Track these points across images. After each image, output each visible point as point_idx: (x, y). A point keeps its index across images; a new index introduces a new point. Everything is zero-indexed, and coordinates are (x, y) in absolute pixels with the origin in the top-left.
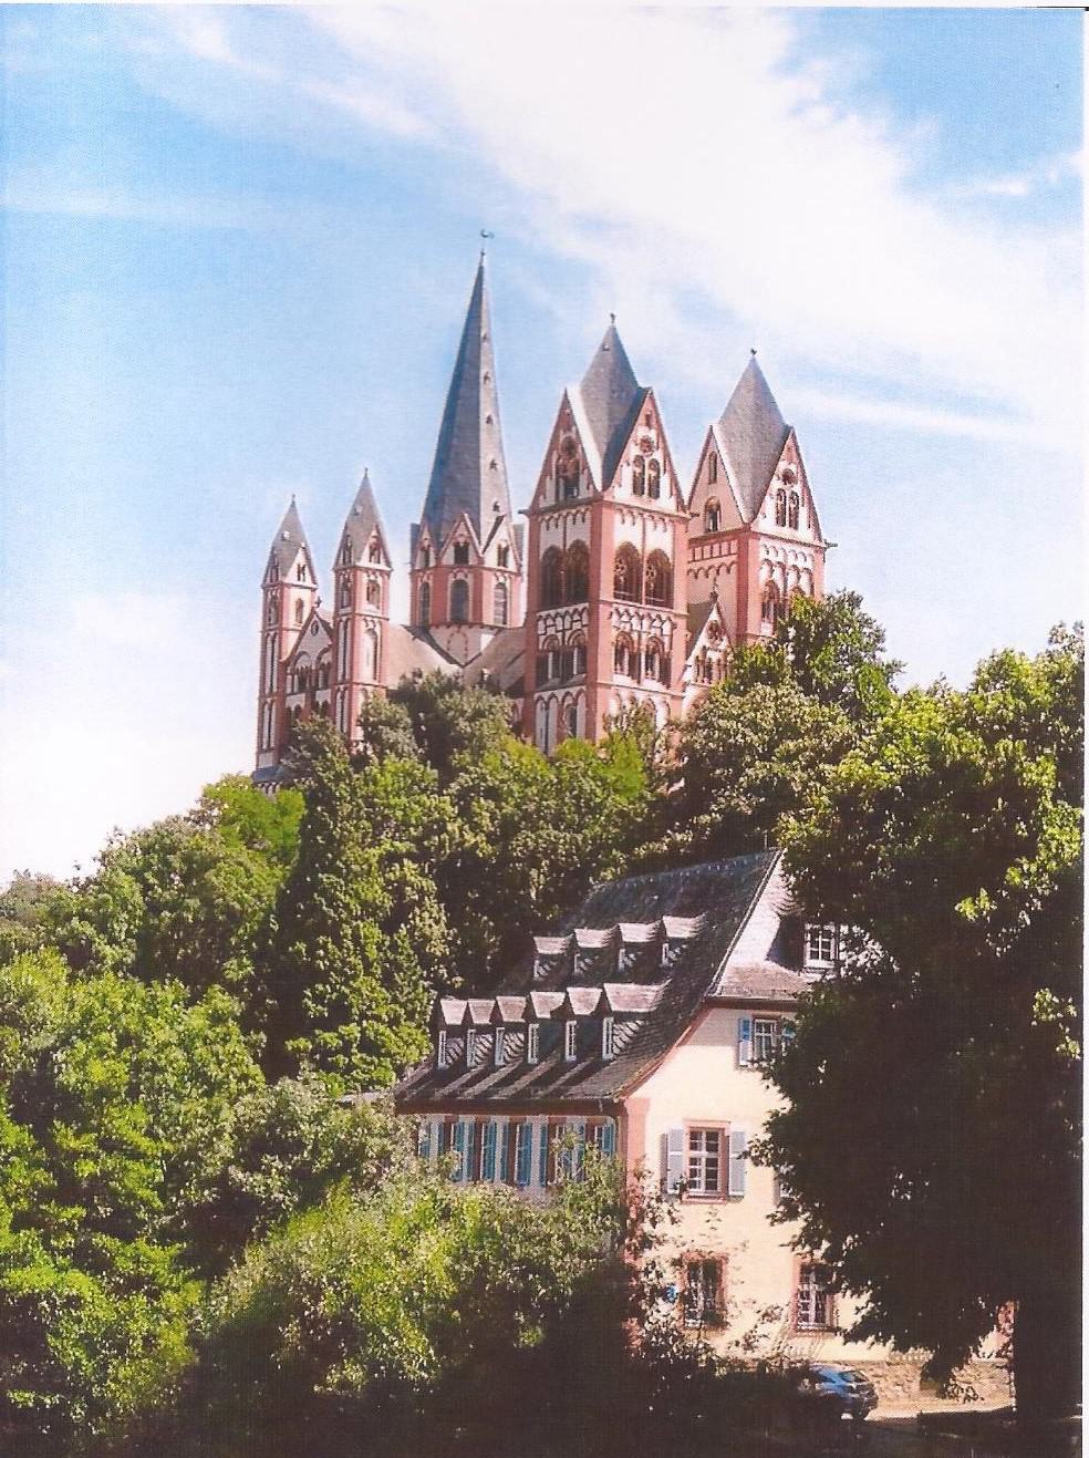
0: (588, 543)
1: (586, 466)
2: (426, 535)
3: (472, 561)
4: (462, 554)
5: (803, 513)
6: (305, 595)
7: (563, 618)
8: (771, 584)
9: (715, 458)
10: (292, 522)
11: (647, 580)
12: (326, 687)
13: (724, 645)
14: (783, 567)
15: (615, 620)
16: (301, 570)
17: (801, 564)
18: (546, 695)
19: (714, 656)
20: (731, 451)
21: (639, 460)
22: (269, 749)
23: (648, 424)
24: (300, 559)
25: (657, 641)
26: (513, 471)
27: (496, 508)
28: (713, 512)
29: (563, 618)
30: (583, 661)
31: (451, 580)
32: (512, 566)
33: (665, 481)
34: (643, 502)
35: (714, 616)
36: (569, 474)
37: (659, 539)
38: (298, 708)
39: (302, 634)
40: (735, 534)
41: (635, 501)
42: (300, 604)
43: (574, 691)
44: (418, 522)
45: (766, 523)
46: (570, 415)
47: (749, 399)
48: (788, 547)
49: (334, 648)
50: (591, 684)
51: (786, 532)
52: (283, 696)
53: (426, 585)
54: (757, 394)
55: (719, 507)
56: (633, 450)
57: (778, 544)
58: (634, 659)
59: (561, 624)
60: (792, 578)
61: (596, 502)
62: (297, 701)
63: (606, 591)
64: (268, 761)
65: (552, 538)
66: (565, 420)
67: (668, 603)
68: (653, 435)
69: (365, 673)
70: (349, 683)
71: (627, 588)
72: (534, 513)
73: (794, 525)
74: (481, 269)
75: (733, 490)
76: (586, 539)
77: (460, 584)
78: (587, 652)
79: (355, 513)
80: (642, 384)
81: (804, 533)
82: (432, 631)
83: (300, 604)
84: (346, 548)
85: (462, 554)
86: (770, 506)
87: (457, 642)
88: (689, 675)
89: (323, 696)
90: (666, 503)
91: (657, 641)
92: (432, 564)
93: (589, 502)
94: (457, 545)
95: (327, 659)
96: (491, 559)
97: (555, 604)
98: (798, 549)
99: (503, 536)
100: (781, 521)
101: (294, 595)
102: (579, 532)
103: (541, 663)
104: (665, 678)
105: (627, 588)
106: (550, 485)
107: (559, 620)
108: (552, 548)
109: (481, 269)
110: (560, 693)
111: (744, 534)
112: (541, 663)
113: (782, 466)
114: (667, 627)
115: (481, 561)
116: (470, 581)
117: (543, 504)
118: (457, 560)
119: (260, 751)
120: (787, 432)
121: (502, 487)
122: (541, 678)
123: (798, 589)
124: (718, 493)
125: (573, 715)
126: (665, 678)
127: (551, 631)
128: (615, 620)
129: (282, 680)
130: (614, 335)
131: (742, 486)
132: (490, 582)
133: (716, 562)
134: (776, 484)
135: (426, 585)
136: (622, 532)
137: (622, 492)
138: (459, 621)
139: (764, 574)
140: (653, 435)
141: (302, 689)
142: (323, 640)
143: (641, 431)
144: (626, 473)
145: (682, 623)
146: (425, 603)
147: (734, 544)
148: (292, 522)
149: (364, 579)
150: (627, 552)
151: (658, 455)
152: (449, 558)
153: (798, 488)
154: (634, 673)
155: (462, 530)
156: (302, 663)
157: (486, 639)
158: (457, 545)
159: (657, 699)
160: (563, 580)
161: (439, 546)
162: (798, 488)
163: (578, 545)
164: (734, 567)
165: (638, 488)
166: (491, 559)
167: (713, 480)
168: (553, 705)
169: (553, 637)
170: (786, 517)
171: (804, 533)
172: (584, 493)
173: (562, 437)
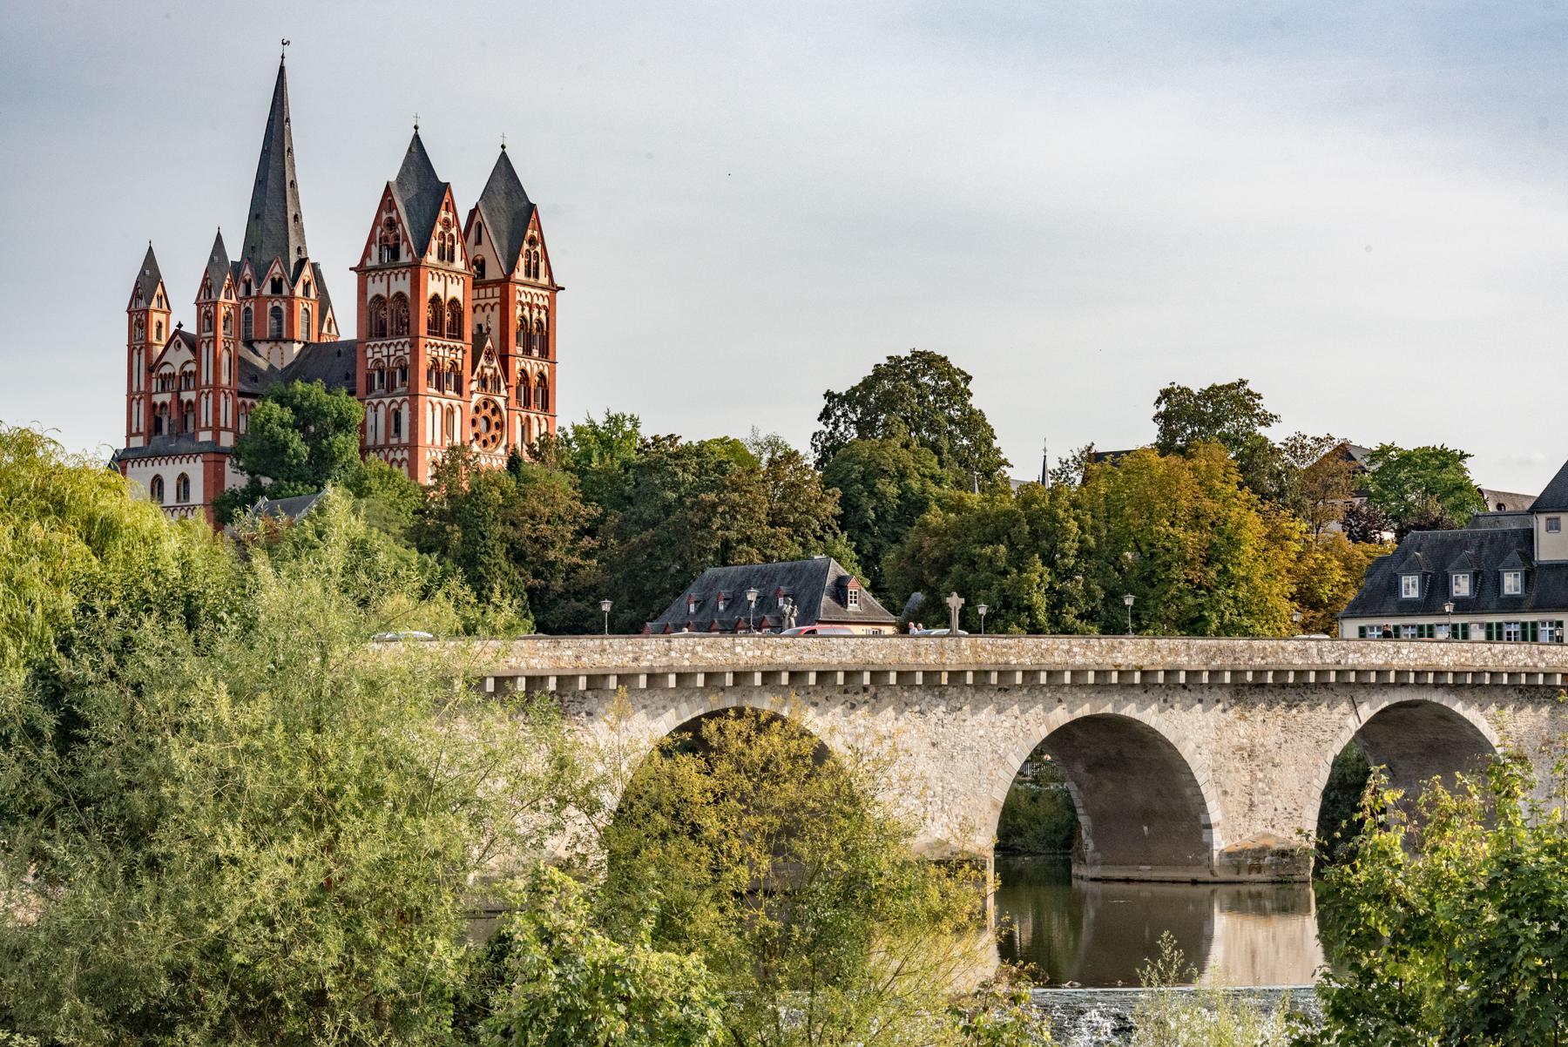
0: (407, 292)
1: (406, 239)
2: (247, 271)
3: (286, 292)
5: (542, 265)
6: (162, 318)
7: (388, 346)
8: (523, 317)
9: (479, 226)
10: (150, 258)
11: (447, 319)
12: (188, 389)
13: (495, 364)
14: (530, 306)
15: (433, 350)
16: (159, 298)
17: (541, 303)
18: (375, 401)
19: (489, 372)
20: (491, 223)
21: (442, 234)
22: (138, 434)
23: (447, 210)
24: (159, 291)
25: (454, 364)
26: (334, 235)
27: (299, 250)
28: (481, 265)
29: (388, 346)
30: (404, 378)
31: (269, 306)
32: (313, 295)
33: (458, 248)
34: (445, 264)
35: (489, 344)
36: (391, 242)
37: (456, 291)
38: (163, 404)
39: (167, 347)
40: (496, 283)
41: (441, 265)
42: (160, 325)
43: (399, 399)
44: (238, 259)
45: (519, 275)
46: (392, 202)
47: (501, 185)
48: (533, 291)
49: (198, 362)
50: (414, 395)
51: (532, 280)
52: (151, 395)
53: (248, 310)
55: (483, 261)
56: (439, 228)
57: (527, 289)
58: (438, 374)
59: (381, 352)
60: (535, 315)
61: (415, 267)
62: (158, 399)
63: (423, 329)
64: (138, 442)
65: (376, 288)
66: (387, 202)
67: (460, 337)
68: (450, 216)
69: (225, 380)
70: (216, 388)
71: (435, 328)
72: (362, 271)
73: (537, 276)
74: (282, 69)
75: (492, 253)
76: (407, 292)
77: (276, 310)
78: (407, 371)
79: (212, 258)
80: (442, 179)
81: (543, 280)
82: (255, 345)
83: (160, 325)
84: (207, 287)
85: (277, 287)
86: (522, 262)
87: (276, 350)
88: (474, 386)
89: (188, 396)
90: (459, 264)
91: (454, 364)
92: (254, 291)
93: (408, 266)
94: (273, 280)
95: (188, 368)
96: (299, 291)
97: (383, 335)
98: (539, 292)
99: (307, 273)
100: (528, 274)
101: (156, 317)
102: (402, 285)
103: (370, 378)
104: (459, 390)
105: (435, 328)
106: (375, 250)
107: (385, 350)
108: (378, 297)
109: (282, 69)
110: (387, 401)
111: (505, 283)
112: (370, 378)
113: (529, 232)
114: (460, 353)
115: (292, 292)
116: (284, 307)
117: (369, 263)
118: (273, 291)
119: (130, 435)
120: (532, 207)
121: (300, 232)
122: (370, 389)
123: (539, 321)
124: (484, 251)
125: (397, 415)
126: (459, 390)
127: (378, 356)
129: (148, 381)
130: (416, 137)
131: (501, 247)
132: (299, 307)
133: (483, 302)
134: (526, 246)
135: (248, 310)
136: (433, 286)
137: (432, 258)
138: (277, 339)
139: (519, 312)
140: (450, 216)
141: (163, 390)
143: (443, 214)
144: (434, 244)
145: (469, 349)
146: (247, 322)
147: (497, 291)
148: (150, 258)
149: (222, 311)
150: (436, 298)
151: (454, 231)
152: (267, 290)
153: (539, 249)
154: (438, 388)
155: (276, 270)
156: (165, 370)
157: (297, 347)
158: (273, 280)
159: (455, 403)
160: (388, 317)
161: (260, 282)
162: (539, 249)
163: (400, 295)
164: (497, 308)
165: (441, 257)
166: (299, 291)
167: (479, 242)
168: (381, 409)
169: (378, 360)
170: (532, 271)
171: (543, 280)
172: (405, 258)
173: (385, 216)
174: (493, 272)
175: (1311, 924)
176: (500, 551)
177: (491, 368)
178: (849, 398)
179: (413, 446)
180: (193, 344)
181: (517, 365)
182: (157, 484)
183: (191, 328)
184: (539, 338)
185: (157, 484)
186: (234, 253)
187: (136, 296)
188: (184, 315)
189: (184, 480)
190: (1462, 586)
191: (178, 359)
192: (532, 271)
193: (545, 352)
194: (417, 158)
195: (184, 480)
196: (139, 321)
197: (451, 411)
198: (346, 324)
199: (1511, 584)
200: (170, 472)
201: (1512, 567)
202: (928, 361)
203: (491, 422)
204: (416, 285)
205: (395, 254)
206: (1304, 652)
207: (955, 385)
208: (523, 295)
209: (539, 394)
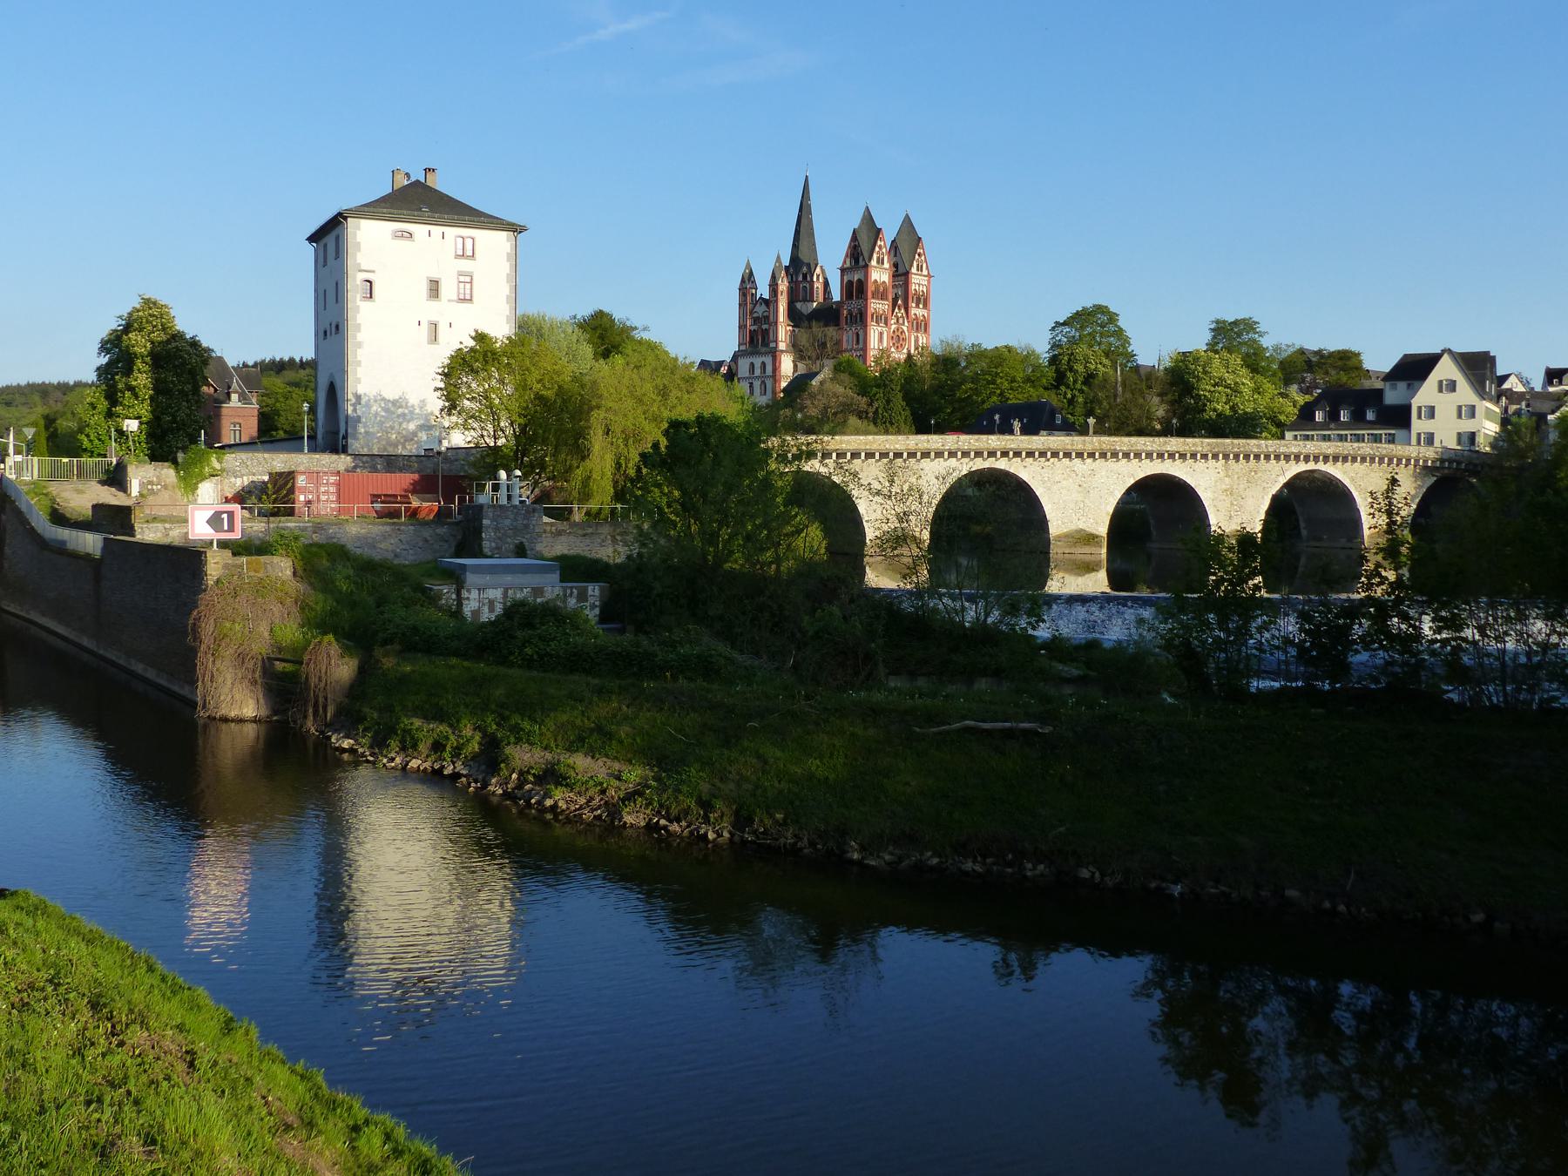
4: (805, 277)
45: (914, 270)
50: (865, 326)
54: (908, 224)
59: (854, 305)
61: (866, 266)
66: (854, 237)
72: (843, 270)
81: (925, 272)
84: (774, 277)
85: (805, 277)
90: (886, 265)
111: (907, 274)
128: (876, 306)
137: (874, 263)
138: (805, 300)
142: (764, 307)
170: (920, 268)
171: (925, 272)
172: (861, 263)
174: (901, 270)
175: (1055, 529)
176: (900, 395)
177: (901, 313)
178: (1064, 324)
179: (865, 349)
180: (767, 302)
181: (914, 311)
182: (752, 365)
183: (766, 296)
184: (923, 300)
185: (752, 365)
186: (786, 262)
187: (743, 281)
188: (763, 291)
189: (764, 364)
190: (1344, 416)
191: (760, 309)
192: (920, 268)
193: (925, 306)
194: (868, 219)
195: (764, 364)
196: (743, 291)
197: (881, 334)
198: (836, 297)
199: (1370, 416)
200: (758, 361)
201: (1370, 406)
202: (1100, 309)
203: (898, 339)
204: (867, 275)
205: (857, 261)
206: (1259, 446)
207: (1113, 318)
208: (917, 282)
209: (922, 326)
